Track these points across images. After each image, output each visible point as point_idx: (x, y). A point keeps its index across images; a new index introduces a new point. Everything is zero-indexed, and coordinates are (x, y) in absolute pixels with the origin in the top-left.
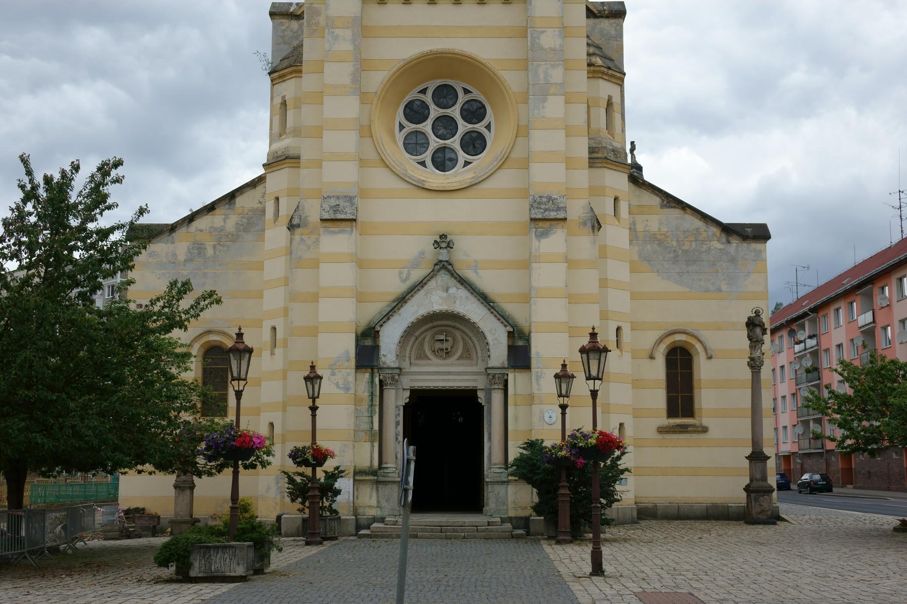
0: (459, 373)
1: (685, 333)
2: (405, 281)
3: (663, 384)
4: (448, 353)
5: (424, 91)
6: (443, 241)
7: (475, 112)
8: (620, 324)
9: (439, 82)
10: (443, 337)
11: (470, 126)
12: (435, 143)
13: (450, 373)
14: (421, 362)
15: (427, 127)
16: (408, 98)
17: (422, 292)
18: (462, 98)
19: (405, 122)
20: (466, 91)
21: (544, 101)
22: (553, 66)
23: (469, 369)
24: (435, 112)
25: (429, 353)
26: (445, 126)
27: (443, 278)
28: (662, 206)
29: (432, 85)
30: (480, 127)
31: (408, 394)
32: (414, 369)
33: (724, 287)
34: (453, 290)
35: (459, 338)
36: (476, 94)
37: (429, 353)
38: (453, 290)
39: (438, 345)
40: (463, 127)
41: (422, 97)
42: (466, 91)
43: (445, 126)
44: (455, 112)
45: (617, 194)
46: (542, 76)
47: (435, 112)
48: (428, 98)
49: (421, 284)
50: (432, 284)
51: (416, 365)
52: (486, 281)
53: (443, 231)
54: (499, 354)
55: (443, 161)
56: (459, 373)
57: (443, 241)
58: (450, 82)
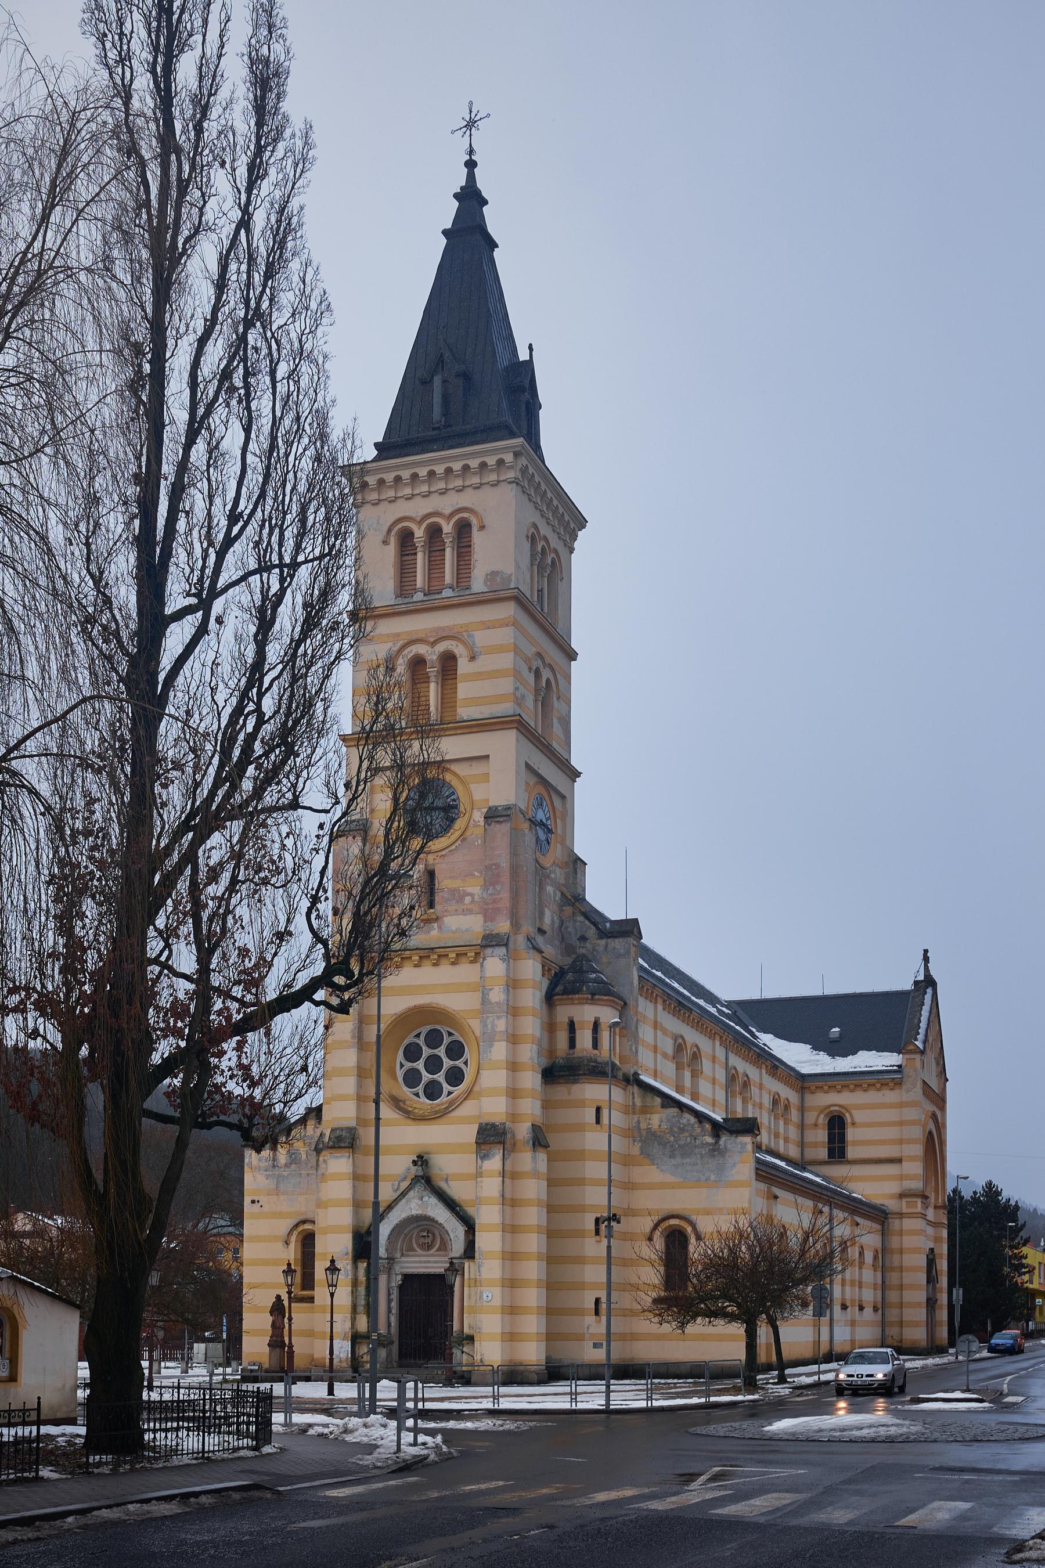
0: (436, 1262)
2: (396, 1191)
4: (429, 1247)
5: (418, 1036)
6: (422, 1161)
7: (456, 1050)
9: (429, 1028)
11: (452, 1063)
12: (426, 1077)
14: (411, 1253)
15: (420, 1065)
16: (406, 1042)
17: (404, 1201)
18: (446, 1040)
19: (404, 1062)
20: (450, 1034)
21: (491, 1046)
22: (499, 1018)
24: (426, 1052)
26: (433, 1065)
27: (418, 1188)
28: (663, 1106)
29: (424, 1030)
30: (459, 1063)
31: (399, 1277)
32: (404, 1259)
34: (426, 1199)
35: (437, 1234)
36: (457, 1037)
38: (426, 1199)
39: (422, 1240)
40: (447, 1063)
41: (416, 1040)
42: (450, 1034)
43: (433, 1065)
44: (441, 1052)
45: (599, 1104)
46: (490, 1026)
47: (426, 1052)
48: (421, 1041)
49: (403, 1194)
50: (411, 1194)
51: (408, 1256)
52: (457, 1190)
53: (419, 1150)
54: (458, 1247)
55: (433, 1091)
56: (436, 1262)
57: (422, 1161)
58: (438, 1027)
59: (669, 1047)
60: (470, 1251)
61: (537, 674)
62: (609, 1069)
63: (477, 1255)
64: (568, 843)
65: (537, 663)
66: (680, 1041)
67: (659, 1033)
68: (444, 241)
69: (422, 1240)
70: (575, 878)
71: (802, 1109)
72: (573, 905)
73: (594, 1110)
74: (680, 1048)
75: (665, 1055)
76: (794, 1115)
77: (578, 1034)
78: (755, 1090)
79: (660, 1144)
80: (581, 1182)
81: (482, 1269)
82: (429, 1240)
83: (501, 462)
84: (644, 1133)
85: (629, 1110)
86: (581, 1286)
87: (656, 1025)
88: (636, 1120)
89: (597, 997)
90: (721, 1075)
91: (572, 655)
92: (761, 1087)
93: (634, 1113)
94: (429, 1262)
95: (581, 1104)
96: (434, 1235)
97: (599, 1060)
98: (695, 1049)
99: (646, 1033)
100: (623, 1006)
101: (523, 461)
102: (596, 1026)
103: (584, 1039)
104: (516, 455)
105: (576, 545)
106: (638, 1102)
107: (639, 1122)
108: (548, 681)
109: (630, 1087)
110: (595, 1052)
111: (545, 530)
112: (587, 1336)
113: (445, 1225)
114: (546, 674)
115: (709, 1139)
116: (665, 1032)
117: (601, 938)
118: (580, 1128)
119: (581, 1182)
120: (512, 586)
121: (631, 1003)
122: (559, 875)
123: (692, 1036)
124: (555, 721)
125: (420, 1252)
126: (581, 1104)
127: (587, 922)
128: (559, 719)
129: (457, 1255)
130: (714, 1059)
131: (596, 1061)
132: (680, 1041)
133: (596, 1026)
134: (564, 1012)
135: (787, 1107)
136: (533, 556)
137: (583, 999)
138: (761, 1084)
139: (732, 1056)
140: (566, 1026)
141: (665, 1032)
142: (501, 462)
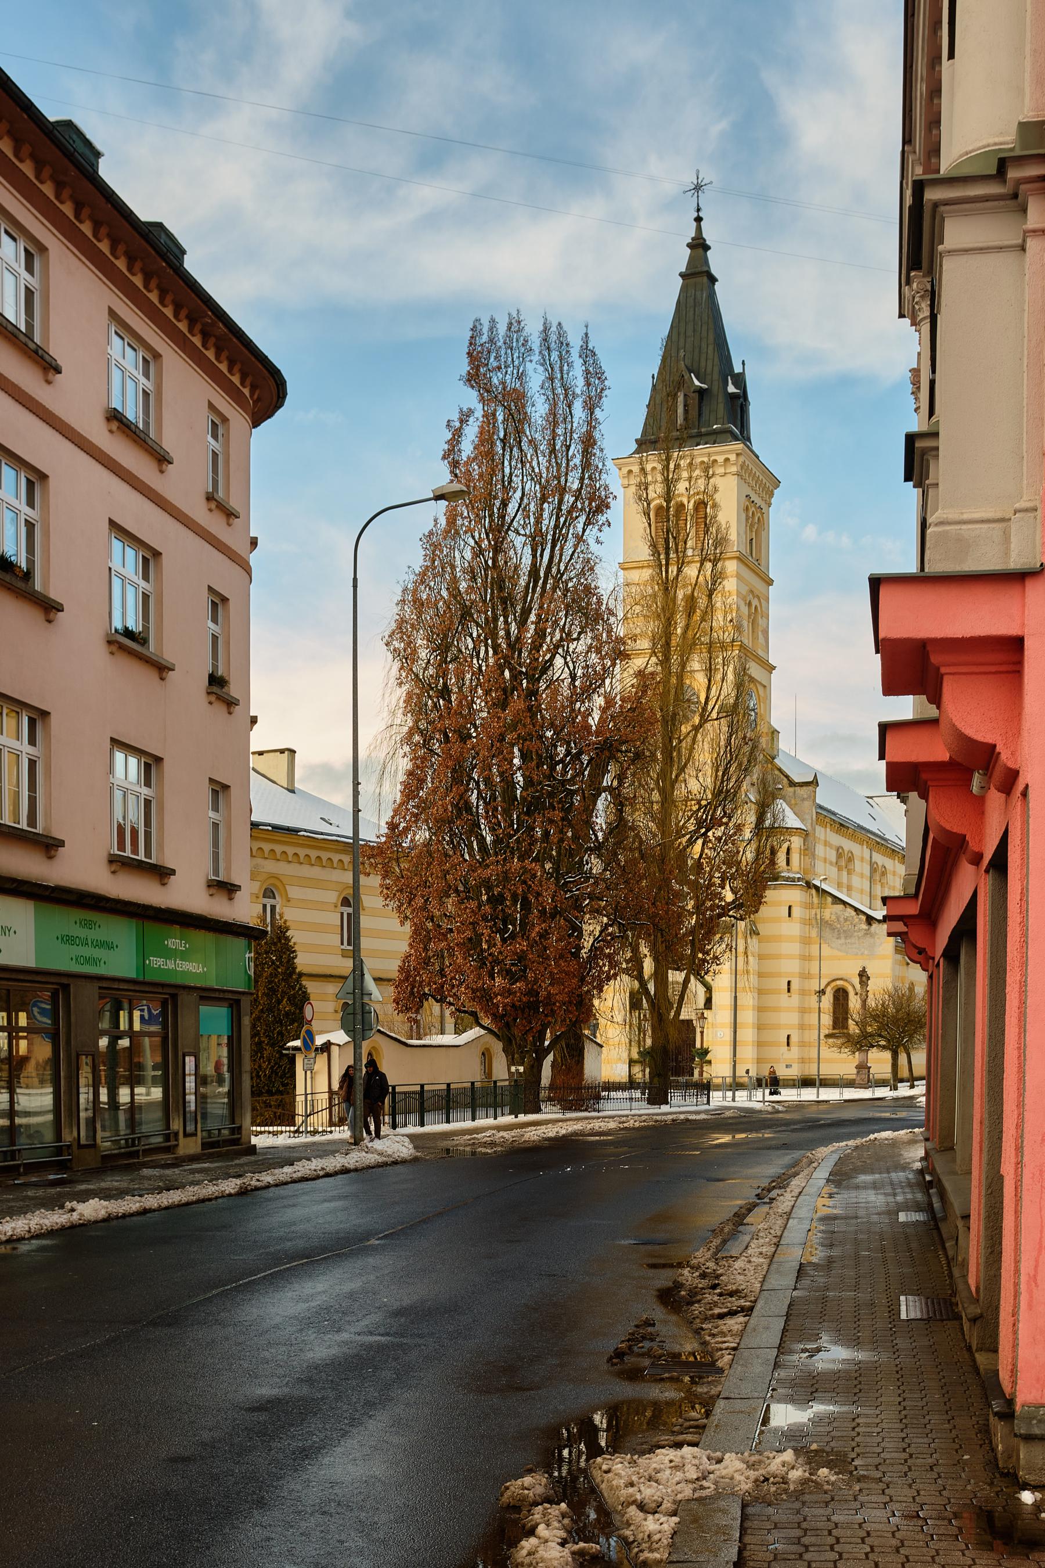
1: (841, 979)
60: (708, 1003)
61: (750, 604)
63: (713, 1007)
68: (680, 281)
70: (772, 744)
74: (840, 854)
75: (831, 863)
78: (890, 876)
80: (777, 957)
81: (717, 1017)
83: (727, 460)
85: (809, 906)
86: (778, 1027)
88: (814, 913)
91: (770, 582)
93: (812, 908)
95: (778, 904)
98: (850, 855)
99: (820, 850)
101: (741, 459)
104: (738, 455)
105: (773, 500)
108: (756, 607)
111: (754, 497)
114: (755, 602)
115: (864, 926)
116: (831, 846)
117: (790, 786)
118: (777, 920)
119: (777, 957)
120: (735, 550)
123: (848, 845)
124: (760, 633)
126: (778, 904)
128: (762, 631)
130: (862, 859)
136: (747, 520)
138: (894, 872)
141: (831, 846)
142: (727, 460)
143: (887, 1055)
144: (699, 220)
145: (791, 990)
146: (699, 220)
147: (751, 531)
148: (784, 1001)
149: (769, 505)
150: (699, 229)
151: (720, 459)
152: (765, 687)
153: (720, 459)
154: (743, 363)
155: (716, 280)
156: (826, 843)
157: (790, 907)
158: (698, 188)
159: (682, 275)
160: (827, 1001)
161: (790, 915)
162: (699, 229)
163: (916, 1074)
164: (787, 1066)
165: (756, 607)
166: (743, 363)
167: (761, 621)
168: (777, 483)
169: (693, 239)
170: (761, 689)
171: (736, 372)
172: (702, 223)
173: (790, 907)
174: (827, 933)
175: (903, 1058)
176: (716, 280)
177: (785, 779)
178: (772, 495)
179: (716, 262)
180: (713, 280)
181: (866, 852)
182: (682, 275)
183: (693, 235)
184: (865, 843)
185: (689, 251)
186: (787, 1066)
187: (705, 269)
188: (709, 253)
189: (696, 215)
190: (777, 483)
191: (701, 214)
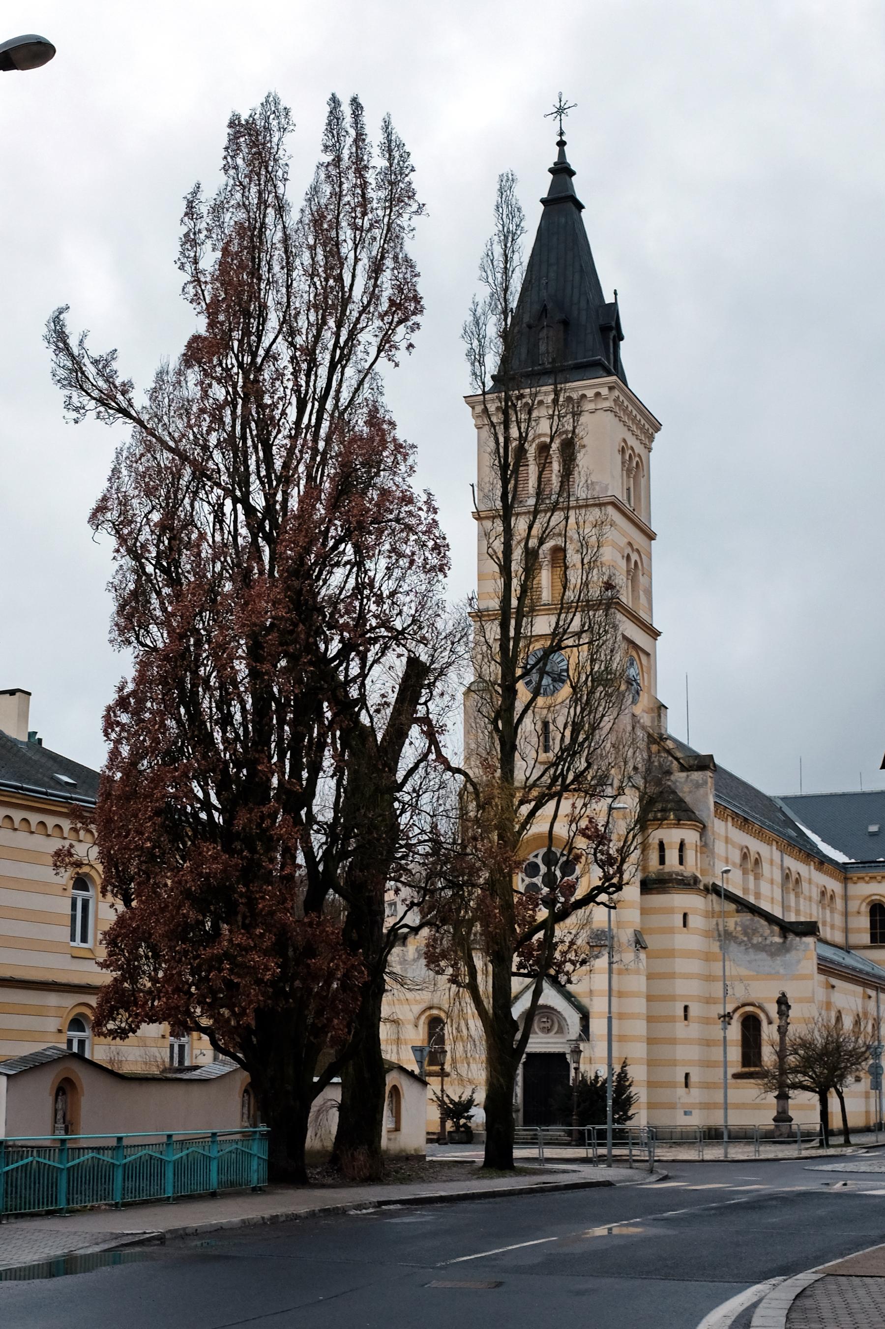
3: (740, 1043)
4: (549, 1030)
5: (536, 856)
8: (687, 1004)
10: (545, 1020)
13: (548, 1043)
23: (561, 1040)
25: (537, 1030)
28: (738, 911)
33: (782, 971)
35: (555, 1020)
37: (537, 1030)
39: (543, 1025)
41: (535, 860)
48: (539, 861)
59: (736, 857)
61: (628, 558)
62: (692, 882)
64: (653, 693)
65: (628, 550)
66: (745, 850)
67: (730, 846)
69: (543, 1025)
70: (659, 721)
71: (846, 898)
72: (659, 744)
73: (682, 916)
76: (839, 903)
77: (667, 852)
78: (805, 885)
79: (735, 942)
80: (671, 976)
82: (548, 1025)
84: (722, 933)
85: (710, 914)
86: (673, 1063)
87: (727, 840)
89: (682, 822)
90: (778, 876)
92: (810, 882)
93: (713, 917)
94: (548, 1043)
95: (671, 911)
96: (553, 1021)
97: (685, 874)
98: (757, 856)
99: (720, 848)
100: (703, 829)
102: (682, 846)
103: (672, 856)
106: (717, 908)
107: (717, 924)
108: (636, 562)
109: (709, 896)
110: (682, 867)
112: (679, 1106)
113: (563, 1013)
114: (634, 557)
115: (778, 939)
116: (734, 845)
117: (682, 771)
118: (671, 931)
119: (671, 976)
121: (709, 825)
122: (646, 719)
124: (641, 593)
125: (541, 1034)
127: (670, 758)
128: (644, 591)
129: (574, 1038)
130: (772, 862)
131: (682, 875)
132: (745, 850)
133: (682, 846)
134: (656, 835)
135: (832, 897)
137: (671, 824)
138: (810, 879)
139: (786, 857)
140: (657, 847)
141: (734, 845)
143: (815, 1098)
144: (561, 144)
145: (689, 1017)
146: (561, 144)
147: (628, 477)
148: (681, 1030)
149: (650, 450)
150: (562, 154)
151: (590, 393)
152: (648, 654)
153: (590, 393)
154: (615, 293)
155: (583, 207)
156: (727, 840)
157: (685, 915)
158: (560, 111)
159: (543, 201)
160: (735, 1031)
161: (685, 925)
162: (562, 154)
163: (851, 1123)
164: (686, 1113)
165: (636, 562)
166: (615, 293)
167: (642, 580)
168: (657, 426)
169: (555, 164)
170: (643, 658)
171: (607, 302)
172: (566, 148)
173: (685, 915)
174: (733, 947)
175: (834, 1103)
176: (583, 207)
177: (675, 762)
178: (651, 438)
179: (580, 187)
180: (580, 207)
181: (777, 855)
182: (543, 201)
183: (556, 160)
184: (774, 843)
185: (551, 176)
186: (686, 1113)
187: (568, 193)
188: (574, 178)
189: (559, 139)
190: (657, 426)
191: (564, 138)
